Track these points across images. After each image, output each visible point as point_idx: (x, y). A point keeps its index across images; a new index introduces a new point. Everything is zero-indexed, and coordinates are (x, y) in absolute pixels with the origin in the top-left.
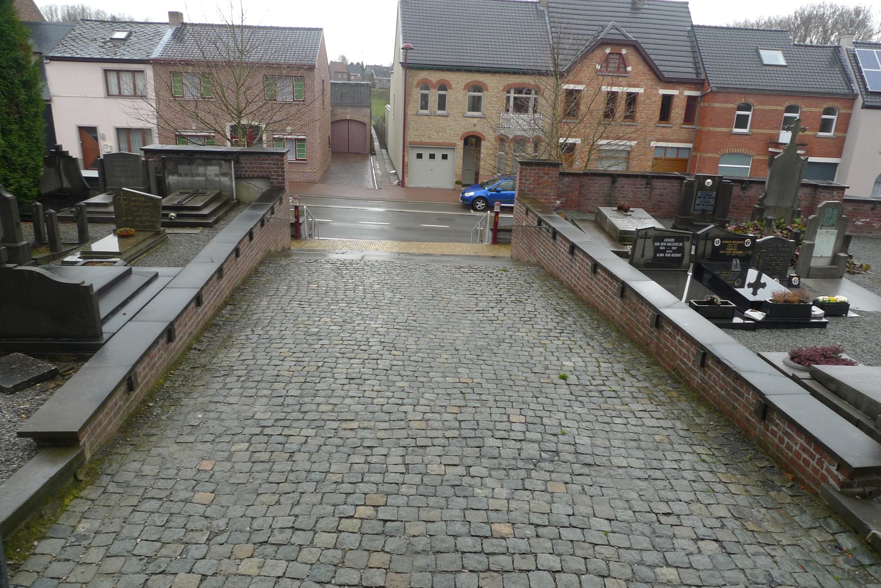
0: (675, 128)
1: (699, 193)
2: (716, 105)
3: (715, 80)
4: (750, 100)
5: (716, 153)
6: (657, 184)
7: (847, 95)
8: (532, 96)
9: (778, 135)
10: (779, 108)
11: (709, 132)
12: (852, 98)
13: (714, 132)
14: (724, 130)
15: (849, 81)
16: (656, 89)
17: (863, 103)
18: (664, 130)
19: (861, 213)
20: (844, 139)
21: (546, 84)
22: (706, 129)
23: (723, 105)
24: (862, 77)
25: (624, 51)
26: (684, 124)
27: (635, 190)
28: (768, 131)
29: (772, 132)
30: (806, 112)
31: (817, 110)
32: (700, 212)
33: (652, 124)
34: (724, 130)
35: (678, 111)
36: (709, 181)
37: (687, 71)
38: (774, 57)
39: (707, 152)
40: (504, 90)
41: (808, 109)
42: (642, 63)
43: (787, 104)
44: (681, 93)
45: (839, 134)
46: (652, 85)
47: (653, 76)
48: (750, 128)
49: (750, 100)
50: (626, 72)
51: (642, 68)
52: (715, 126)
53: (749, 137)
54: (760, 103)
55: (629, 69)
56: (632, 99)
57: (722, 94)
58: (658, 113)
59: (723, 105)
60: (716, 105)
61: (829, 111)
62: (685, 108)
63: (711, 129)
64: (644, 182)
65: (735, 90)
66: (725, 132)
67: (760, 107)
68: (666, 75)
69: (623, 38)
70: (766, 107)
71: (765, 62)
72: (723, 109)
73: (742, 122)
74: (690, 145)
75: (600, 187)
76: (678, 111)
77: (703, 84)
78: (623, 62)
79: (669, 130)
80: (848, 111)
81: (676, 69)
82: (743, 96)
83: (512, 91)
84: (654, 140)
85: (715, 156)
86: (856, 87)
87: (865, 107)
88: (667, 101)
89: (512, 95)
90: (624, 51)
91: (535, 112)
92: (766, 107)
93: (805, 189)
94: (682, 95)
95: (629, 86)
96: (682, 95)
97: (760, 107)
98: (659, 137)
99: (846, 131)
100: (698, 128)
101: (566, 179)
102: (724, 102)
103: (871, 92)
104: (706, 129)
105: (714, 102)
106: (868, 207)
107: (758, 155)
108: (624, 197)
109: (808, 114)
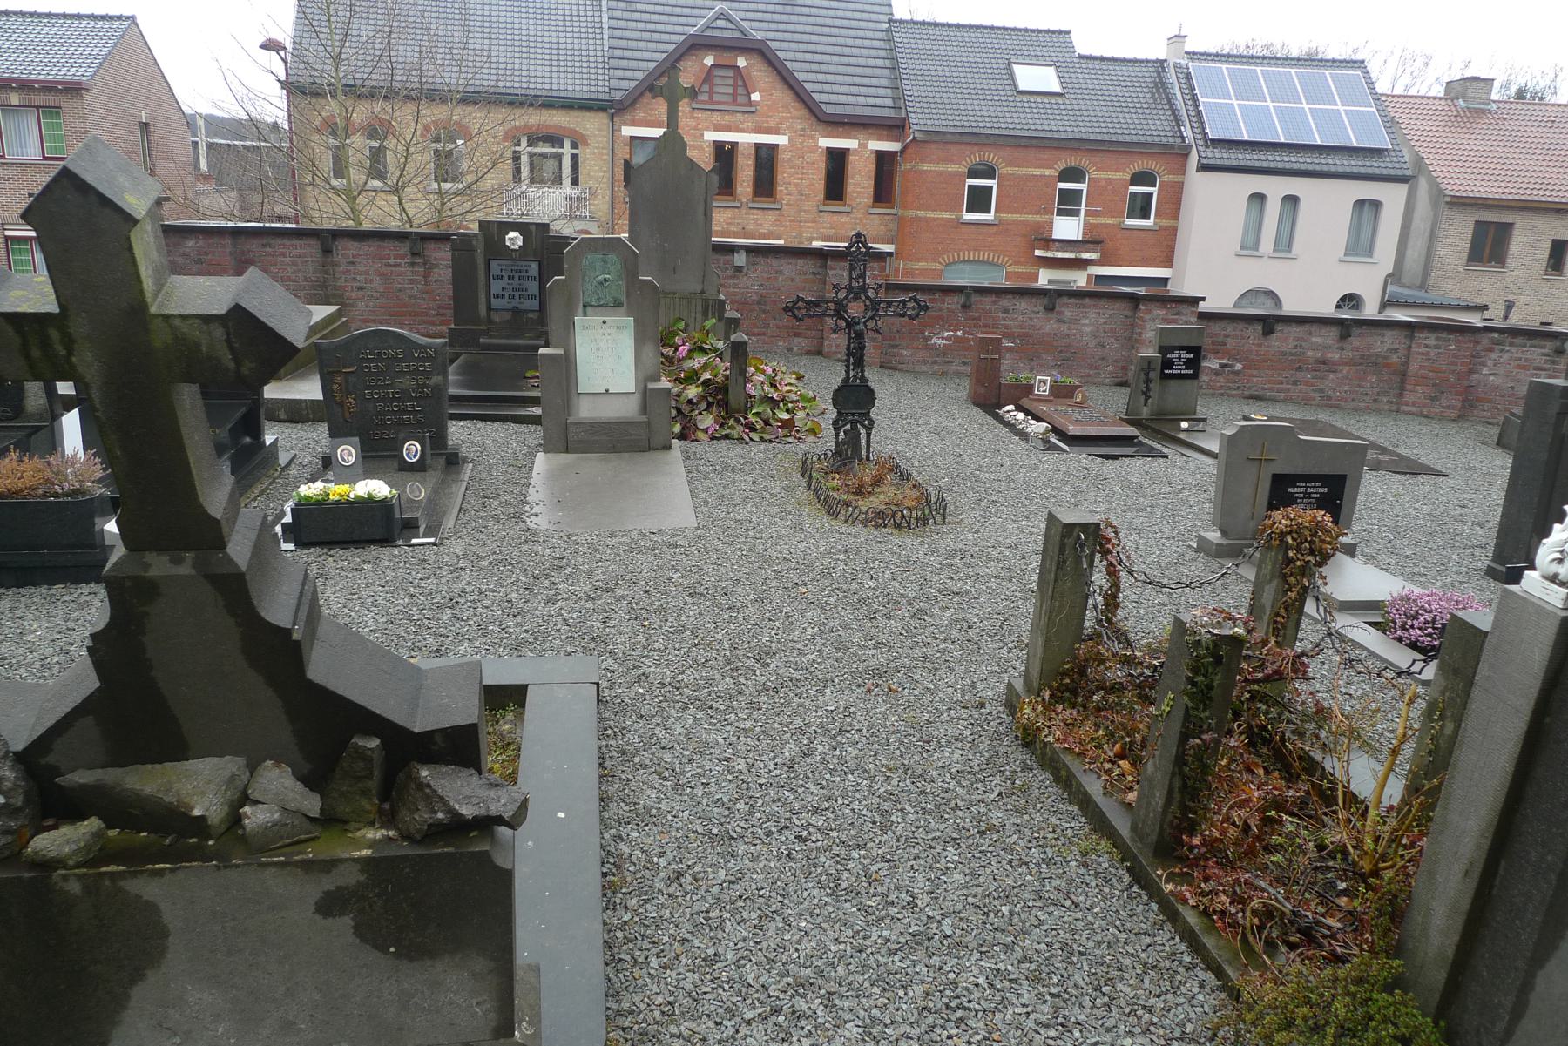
0: (858, 214)
1: (495, 267)
2: (926, 167)
3: (920, 119)
4: (991, 157)
5: (935, 260)
6: (438, 255)
7: (1172, 146)
8: (567, 150)
9: (1051, 224)
10: (1047, 172)
12: (1183, 153)
13: (926, 220)
14: (946, 215)
15: (1178, 123)
16: (812, 137)
17: (1199, 160)
18: (835, 217)
19: (941, 318)
20: (1174, 230)
21: (592, 125)
22: (911, 213)
23: (941, 167)
24: (1199, 114)
25: (742, 62)
26: (873, 207)
27: (385, 270)
28: (1030, 218)
29: (1038, 218)
31: (1118, 175)
32: (507, 316)
33: (810, 205)
34: (946, 215)
35: (860, 181)
36: (512, 234)
37: (877, 102)
38: (1036, 77)
39: (918, 260)
40: (505, 138)
41: (1103, 175)
42: (779, 85)
43: (1062, 165)
44: (863, 146)
45: (1165, 223)
46: (803, 130)
47: (805, 112)
48: (996, 212)
49: (991, 157)
50: (750, 103)
51: (782, 95)
52: (928, 208)
53: (995, 228)
54: (1010, 164)
55: (755, 97)
56: (766, 158)
57: (933, 146)
58: (820, 185)
59: (941, 167)
60: (926, 167)
61: (1139, 179)
62: (873, 174)
63: (921, 213)
64: (404, 249)
65: (958, 138)
67: (1010, 171)
68: (829, 109)
69: (737, 35)
70: (1023, 171)
71: (1022, 87)
72: (940, 174)
73: (979, 200)
75: (294, 263)
76: (860, 181)
77: (903, 127)
78: (742, 82)
79: (845, 219)
80: (1178, 178)
81: (852, 99)
82: (976, 148)
83: (524, 143)
86: (1187, 132)
87: (1204, 168)
88: (837, 159)
90: (742, 62)
91: (575, 182)
92: (1023, 171)
93: (801, 262)
94: (863, 148)
95: (759, 130)
96: (863, 148)
97: (1010, 171)
98: (831, 232)
99: (1176, 217)
100: (900, 212)
101: (190, 243)
103: (1213, 141)
104: (911, 213)
105: (923, 161)
106: (955, 301)
107: (1016, 263)
108: (360, 289)
109: (1103, 183)
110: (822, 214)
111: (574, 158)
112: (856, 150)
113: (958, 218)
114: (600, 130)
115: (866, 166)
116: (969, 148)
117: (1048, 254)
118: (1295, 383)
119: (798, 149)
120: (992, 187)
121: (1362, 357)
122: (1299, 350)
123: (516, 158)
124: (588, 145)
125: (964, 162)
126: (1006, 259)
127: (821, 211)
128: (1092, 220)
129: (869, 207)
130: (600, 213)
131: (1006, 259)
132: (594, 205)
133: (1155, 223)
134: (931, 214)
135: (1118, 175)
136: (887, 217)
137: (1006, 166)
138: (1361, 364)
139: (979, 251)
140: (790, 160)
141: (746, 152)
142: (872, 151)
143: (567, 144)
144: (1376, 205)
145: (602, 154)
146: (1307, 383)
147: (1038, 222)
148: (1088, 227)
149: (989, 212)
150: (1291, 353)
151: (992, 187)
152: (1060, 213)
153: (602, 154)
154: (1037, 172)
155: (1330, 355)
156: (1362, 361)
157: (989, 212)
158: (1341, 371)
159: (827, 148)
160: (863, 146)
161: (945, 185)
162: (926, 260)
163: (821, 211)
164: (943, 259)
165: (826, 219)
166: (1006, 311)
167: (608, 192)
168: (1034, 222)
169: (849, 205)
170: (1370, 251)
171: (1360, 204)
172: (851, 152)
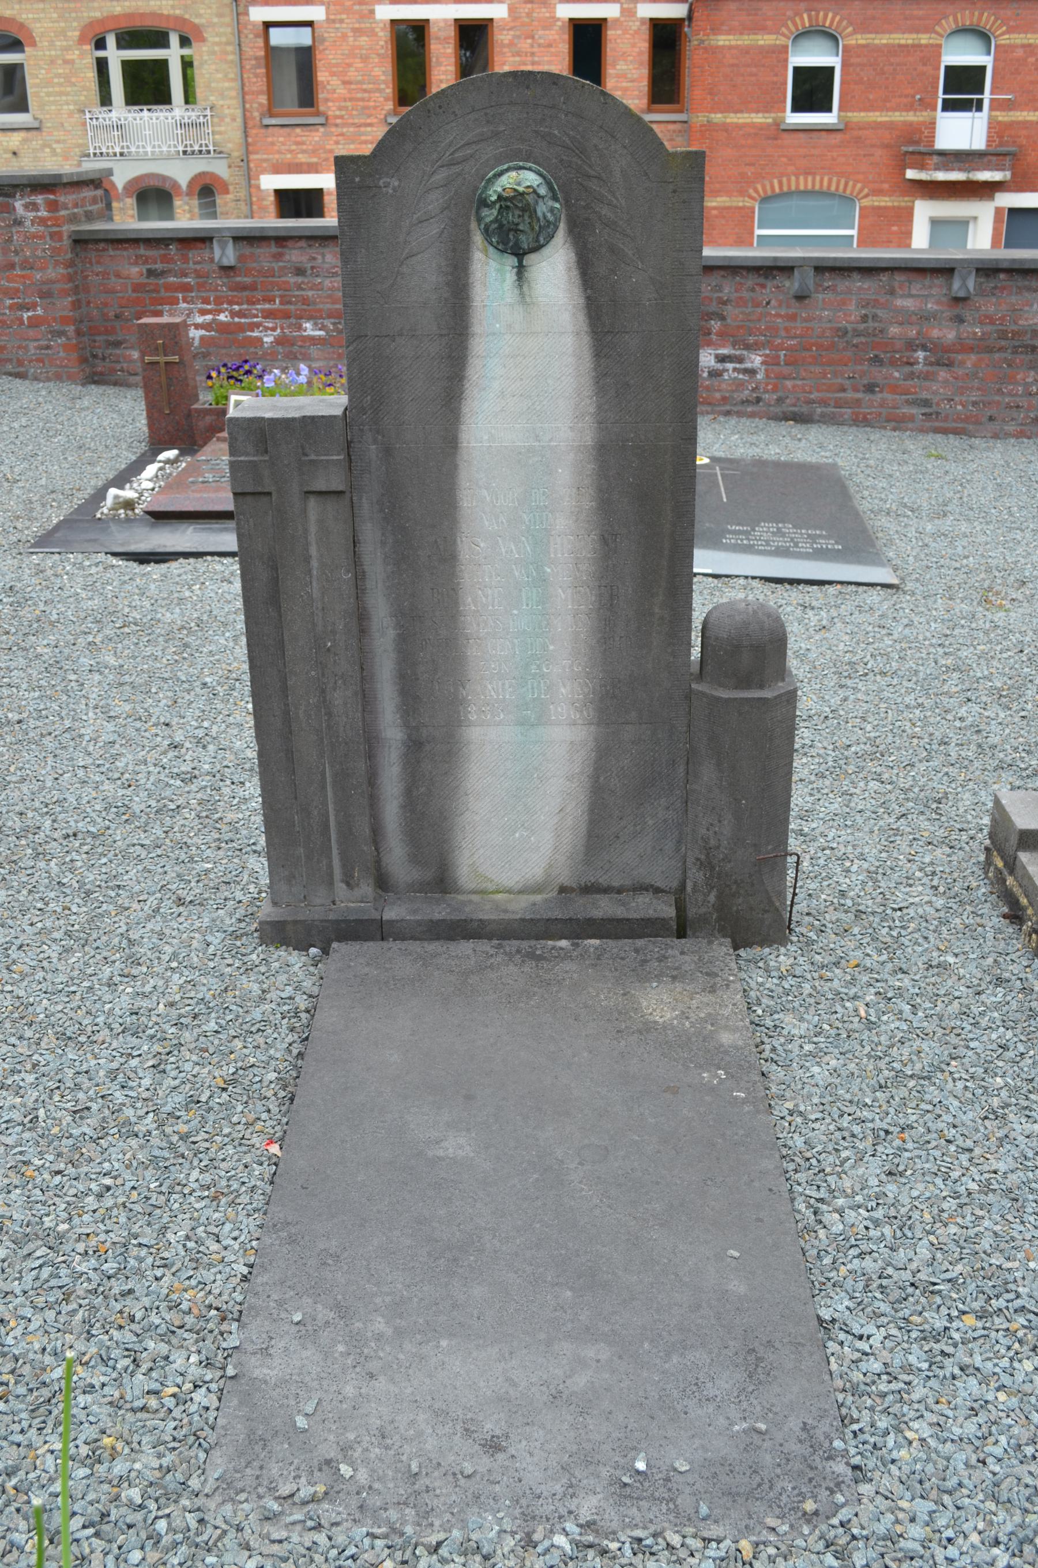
2: (722, 40)
5: (742, 193)
9: (932, 125)
11: (710, 126)
13: (725, 128)
14: (758, 118)
19: (186, 288)
23: (746, 40)
26: (650, 110)
28: (898, 117)
29: (911, 117)
30: (1012, 47)
34: (758, 118)
44: (628, 13)
48: (841, 109)
53: (839, 136)
54: (862, 27)
59: (746, 40)
60: (722, 40)
63: (717, 117)
66: (762, 127)
67: (861, 39)
70: (883, 40)
72: (746, 51)
83: (111, 41)
85: (739, 202)
89: (115, 56)
91: (189, 98)
92: (883, 40)
97: (861, 39)
104: (700, 118)
105: (716, 30)
107: (878, 192)
109: (1020, 53)
111: (187, 64)
112: (616, 20)
113: (777, 124)
114: (220, 15)
115: (633, 45)
117: (923, 176)
118: (870, 388)
119: (523, 25)
120: (831, 70)
121: (1003, 335)
122: (871, 324)
123: (102, 66)
124: (203, 40)
125: (784, 30)
126: (859, 186)
128: (1002, 116)
130: (230, 145)
131: (859, 186)
132: (220, 133)
134: (733, 118)
136: (671, 127)
137: (855, 32)
138: (1001, 349)
139: (814, 174)
140: (511, 44)
141: (442, 34)
142: (643, 21)
143: (174, 40)
145: (226, 53)
146: (894, 389)
147: (911, 124)
148: (995, 129)
149: (829, 110)
150: (857, 333)
151: (831, 70)
152: (949, 106)
153: (226, 53)
154: (906, 39)
155: (935, 333)
156: (1003, 343)
157: (829, 110)
158: (962, 363)
159: (571, 20)
160: (628, 13)
161: (754, 70)
162: (729, 193)
164: (756, 191)
166: (300, 271)
167: (239, 113)
168: (905, 123)
172: (609, 24)
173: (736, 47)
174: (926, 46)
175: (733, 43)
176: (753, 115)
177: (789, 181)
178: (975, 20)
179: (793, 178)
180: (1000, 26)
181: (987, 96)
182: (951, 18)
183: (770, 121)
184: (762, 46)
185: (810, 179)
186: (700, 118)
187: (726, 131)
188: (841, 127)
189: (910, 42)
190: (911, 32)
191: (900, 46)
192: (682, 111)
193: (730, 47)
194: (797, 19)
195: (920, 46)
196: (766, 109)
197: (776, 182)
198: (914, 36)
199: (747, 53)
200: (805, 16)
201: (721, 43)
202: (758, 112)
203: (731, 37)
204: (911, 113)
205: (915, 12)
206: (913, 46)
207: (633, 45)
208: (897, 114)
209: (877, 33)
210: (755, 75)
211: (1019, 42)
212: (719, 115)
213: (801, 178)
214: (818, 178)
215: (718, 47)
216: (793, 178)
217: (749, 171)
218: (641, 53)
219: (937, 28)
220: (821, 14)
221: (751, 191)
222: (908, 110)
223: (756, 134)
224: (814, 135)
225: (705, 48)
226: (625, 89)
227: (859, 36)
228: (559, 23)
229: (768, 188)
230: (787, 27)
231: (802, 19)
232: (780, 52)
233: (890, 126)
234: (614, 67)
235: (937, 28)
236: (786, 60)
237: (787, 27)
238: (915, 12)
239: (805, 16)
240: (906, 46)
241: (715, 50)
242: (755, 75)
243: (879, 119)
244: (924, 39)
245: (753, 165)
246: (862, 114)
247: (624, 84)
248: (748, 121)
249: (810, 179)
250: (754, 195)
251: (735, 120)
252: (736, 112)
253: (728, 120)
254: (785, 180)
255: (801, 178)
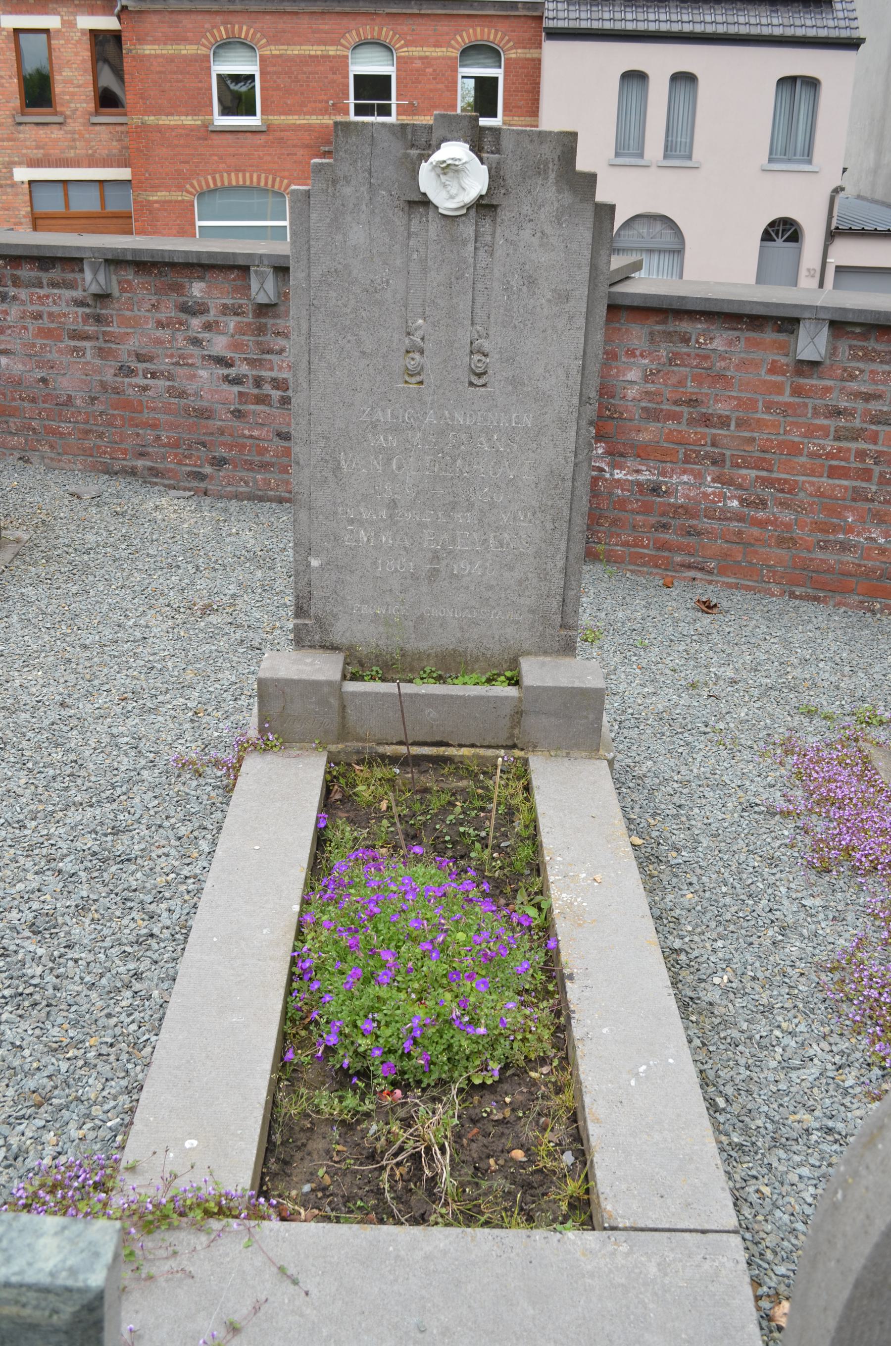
0: (75, 125)
2: (148, 49)
5: (180, 188)
13: (159, 129)
14: (188, 121)
18: (42, 132)
23: (170, 50)
26: (97, 113)
30: (412, 59)
31: (439, 52)
34: (188, 121)
39: (156, 188)
41: (416, 51)
44: (69, 24)
48: (262, 114)
52: (159, 111)
53: (261, 139)
54: (274, 39)
57: (155, 18)
59: (170, 50)
60: (148, 49)
63: (151, 119)
66: (192, 129)
67: (275, 50)
70: (295, 51)
72: (170, 59)
74: (124, 174)
79: (56, 133)
80: (531, 54)
82: (219, 19)
84: (20, 164)
85: (177, 196)
92: (295, 51)
97: (275, 50)
98: (39, 153)
102: (167, 40)
104: (135, 120)
109: (418, 64)
110: (21, 128)
112: (58, 31)
113: (205, 126)
115: (76, 54)
116: (207, 17)
126: (286, 181)
127: (20, 124)
129: (91, 115)
131: (286, 181)
133: (504, 123)
134: (164, 121)
135: (439, 52)
136: (119, 128)
137: (268, 43)
139: (244, 171)
142: (83, 31)
144: (812, 83)
154: (316, 50)
160: (69, 24)
161: (180, 76)
162: (168, 189)
163: (20, 124)
164: (193, 187)
165: (29, 134)
168: (321, 125)
169: (62, 113)
170: (808, 154)
171: (788, 82)
173: (162, 56)
174: (334, 57)
175: (158, 52)
176: (183, 118)
177: (222, 177)
178: (376, 34)
179: (225, 175)
180: (399, 40)
181: (394, 101)
182: (354, 32)
183: (199, 123)
184: (185, 55)
185: (240, 175)
186: (135, 120)
187: (160, 132)
188: (264, 129)
189: (319, 53)
190: (319, 44)
191: (311, 56)
192: (125, 115)
193: (156, 56)
194: (215, 31)
195: (329, 56)
196: (194, 112)
197: (209, 177)
198: (323, 48)
199: (173, 61)
200: (222, 28)
201: (147, 52)
202: (187, 115)
203: (156, 47)
204: (326, 117)
205: (321, 27)
206: (323, 56)
207: (76, 54)
208: (314, 117)
209: (288, 44)
210: (182, 81)
211: (416, 54)
212: (152, 118)
213: (233, 175)
214: (248, 175)
215: (144, 56)
216: (225, 175)
217: (185, 168)
218: (83, 61)
219: (342, 41)
220: (237, 27)
221: (188, 186)
222: (323, 115)
223: (188, 135)
224: (240, 136)
225: (133, 57)
226: (73, 94)
227: (273, 48)
228: (5, 33)
229: (203, 183)
230: (207, 39)
231: (219, 31)
232: (202, 61)
233: (309, 128)
234: (60, 73)
235: (342, 41)
236: (209, 68)
237: (207, 39)
238: (321, 27)
239: (222, 28)
240: (316, 56)
241: (143, 58)
242: (182, 81)
243: (298, 122)
244: (332, 51)
245: (188, 162)
246: (282, 117)
247: (71, 89)
248: (180, 123)
249: (240, 175)
250: (191, 190)
251: (167, 122)
252: (167, 115)
253: (161, 122)
254: (217, 176)
255: (233, 175)
